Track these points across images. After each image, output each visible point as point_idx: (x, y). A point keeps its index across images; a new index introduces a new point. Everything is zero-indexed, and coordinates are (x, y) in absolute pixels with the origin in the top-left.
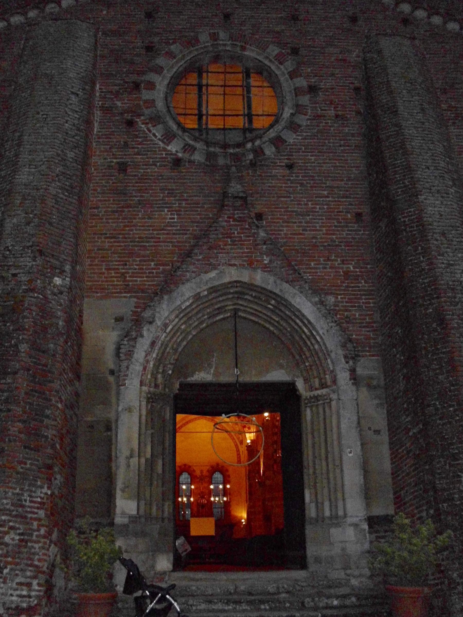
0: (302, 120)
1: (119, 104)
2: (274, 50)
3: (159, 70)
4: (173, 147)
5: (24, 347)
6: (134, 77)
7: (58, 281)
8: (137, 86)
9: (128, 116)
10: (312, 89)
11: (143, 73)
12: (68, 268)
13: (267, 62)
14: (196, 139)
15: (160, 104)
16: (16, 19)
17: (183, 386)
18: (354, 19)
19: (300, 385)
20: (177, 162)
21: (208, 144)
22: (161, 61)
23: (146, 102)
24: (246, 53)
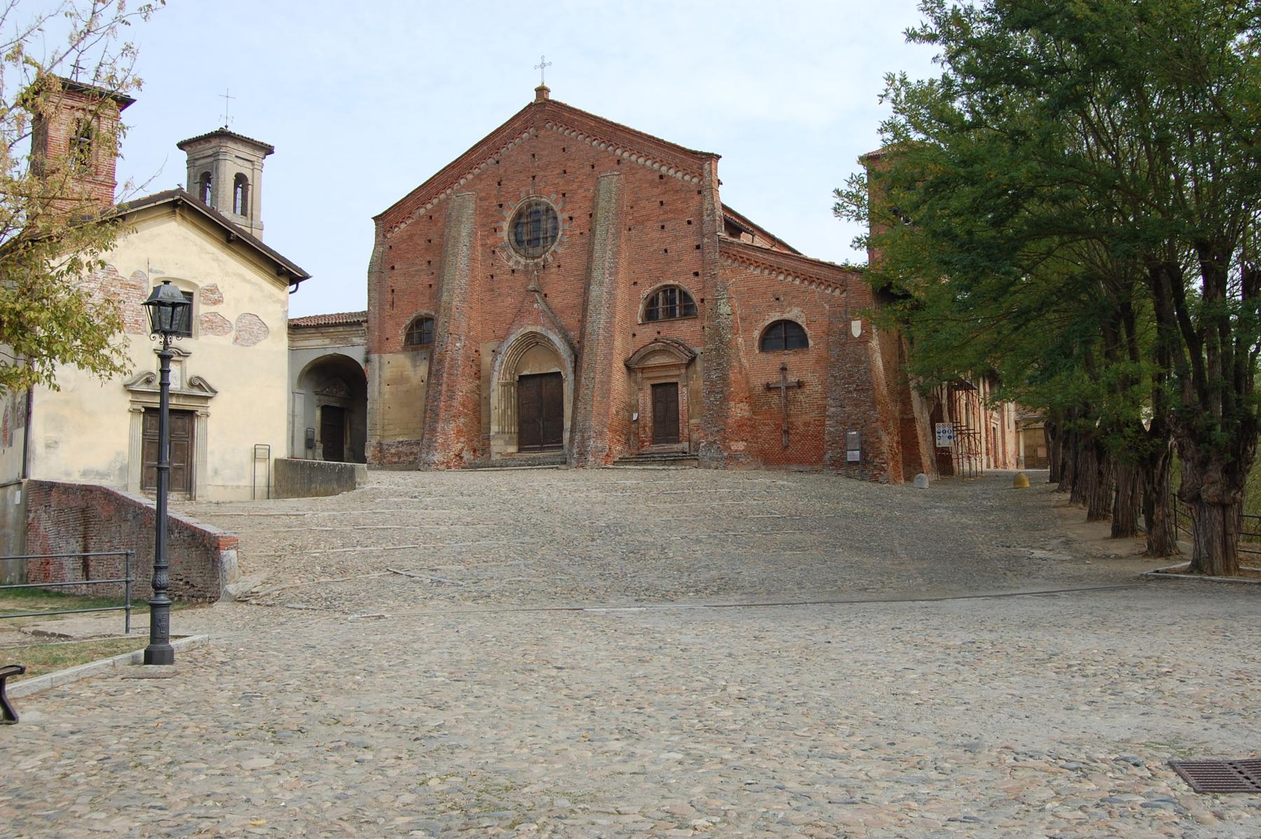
0: (565, 239)
1: (488, 242)
2: (554, 196)
3: (504, 219)
4: (511, 264)
5: (445, 375)
6: (494, 225)
7: (458, 345)
8: (495, 230)
9: (492, 249)
10: (571, 218)
11: (497, 222)
12: (462, 338)
13: (552, 205)
14: (521, 256)
15: (506, 238)
16: (442, 196)
17: (520, 377)
18: (593, 167)
19: (562, 373)
20: (513, 271)
21: (526, 258)
22: (504, 213)
23: (499, 239)
24: (543, 199)
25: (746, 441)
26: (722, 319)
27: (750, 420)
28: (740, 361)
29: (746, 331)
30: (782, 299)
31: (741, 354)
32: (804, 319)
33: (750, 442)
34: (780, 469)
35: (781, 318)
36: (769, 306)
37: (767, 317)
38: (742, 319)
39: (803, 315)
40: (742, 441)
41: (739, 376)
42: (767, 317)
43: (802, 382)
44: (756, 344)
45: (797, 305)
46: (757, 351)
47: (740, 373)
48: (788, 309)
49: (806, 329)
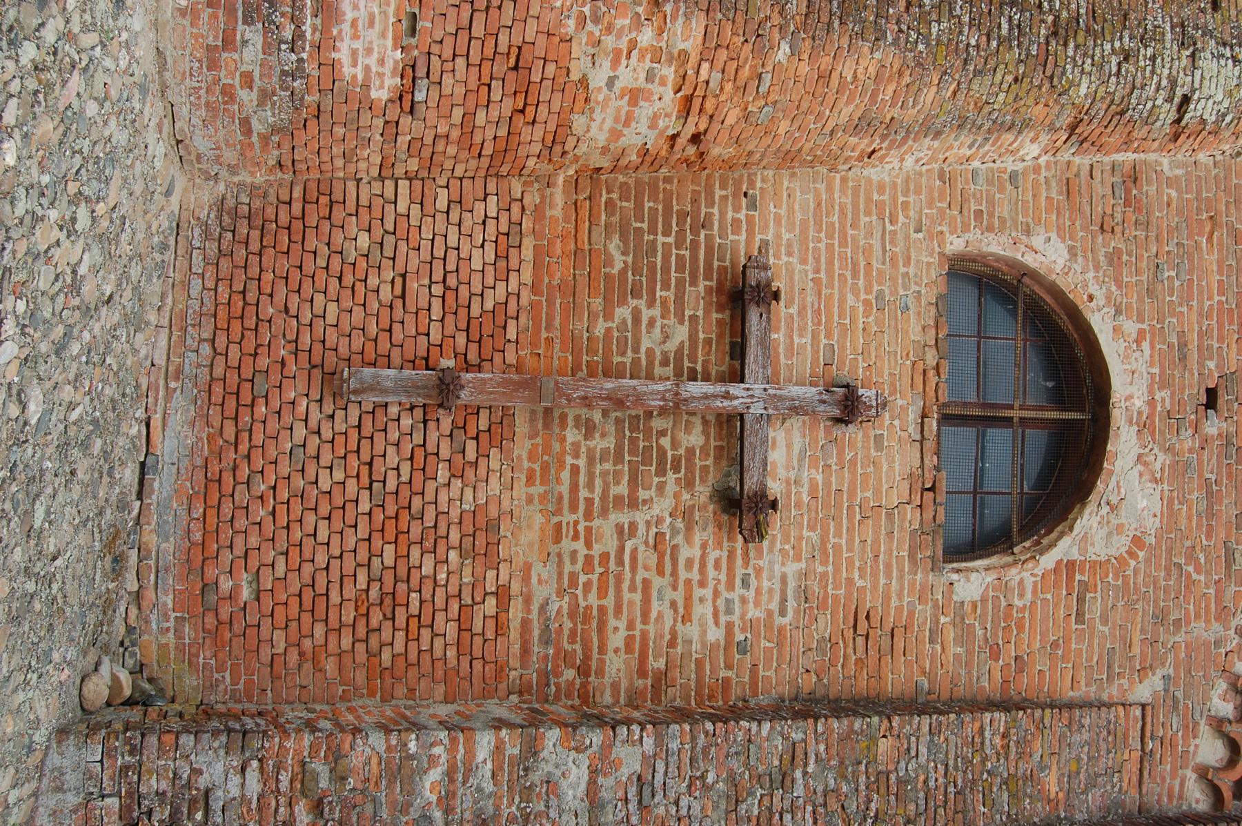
25: (404, 99)
26: (1173, 60)
27: (555, 144)
28: (930, 129)
29: (1068, 188)
30: (1213, 426)
31: (959, 146)
32: (1100, 549)
33: (392, 129)
34: (179, 324)
35: (1118, 416)
36: (1183, 345)
37: (1131, 327)
38: (1134, 176)
39: (1120, 545)
40: (409, 72)
41: (847, 112)
42: (1131, 327)
43: (757, 533)
44: (995, 246)
45: (1170, 514)
46: (955, 245)
47: (861, 126)
48: (1160, 460)
49: (1048, 561)
